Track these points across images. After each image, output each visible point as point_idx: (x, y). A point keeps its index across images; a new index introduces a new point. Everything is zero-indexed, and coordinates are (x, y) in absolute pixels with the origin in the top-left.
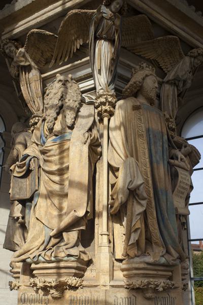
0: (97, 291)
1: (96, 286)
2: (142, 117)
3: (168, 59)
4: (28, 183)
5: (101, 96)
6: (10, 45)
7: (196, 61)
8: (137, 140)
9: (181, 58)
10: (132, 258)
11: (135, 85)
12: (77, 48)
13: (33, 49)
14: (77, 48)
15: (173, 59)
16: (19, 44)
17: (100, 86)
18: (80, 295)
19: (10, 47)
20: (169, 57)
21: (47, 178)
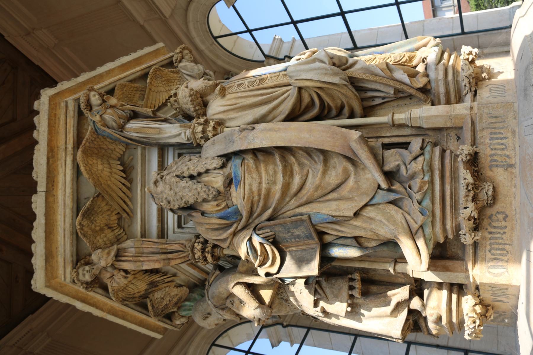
0: (481, 119)
1: (473, 123)
2: (236, 84)
4: (294, 249)
5: (194, 133)
6: (80, 271)
7: (187, 57)
8: (265, 85)
9: (178, 72)
10: (429, 81)
13: (98, 238)
15: (176, 81)
16: (85, 258)
17: (180, 134)
18: (489, 149)
19: (83, 270)
21: (293, 201)
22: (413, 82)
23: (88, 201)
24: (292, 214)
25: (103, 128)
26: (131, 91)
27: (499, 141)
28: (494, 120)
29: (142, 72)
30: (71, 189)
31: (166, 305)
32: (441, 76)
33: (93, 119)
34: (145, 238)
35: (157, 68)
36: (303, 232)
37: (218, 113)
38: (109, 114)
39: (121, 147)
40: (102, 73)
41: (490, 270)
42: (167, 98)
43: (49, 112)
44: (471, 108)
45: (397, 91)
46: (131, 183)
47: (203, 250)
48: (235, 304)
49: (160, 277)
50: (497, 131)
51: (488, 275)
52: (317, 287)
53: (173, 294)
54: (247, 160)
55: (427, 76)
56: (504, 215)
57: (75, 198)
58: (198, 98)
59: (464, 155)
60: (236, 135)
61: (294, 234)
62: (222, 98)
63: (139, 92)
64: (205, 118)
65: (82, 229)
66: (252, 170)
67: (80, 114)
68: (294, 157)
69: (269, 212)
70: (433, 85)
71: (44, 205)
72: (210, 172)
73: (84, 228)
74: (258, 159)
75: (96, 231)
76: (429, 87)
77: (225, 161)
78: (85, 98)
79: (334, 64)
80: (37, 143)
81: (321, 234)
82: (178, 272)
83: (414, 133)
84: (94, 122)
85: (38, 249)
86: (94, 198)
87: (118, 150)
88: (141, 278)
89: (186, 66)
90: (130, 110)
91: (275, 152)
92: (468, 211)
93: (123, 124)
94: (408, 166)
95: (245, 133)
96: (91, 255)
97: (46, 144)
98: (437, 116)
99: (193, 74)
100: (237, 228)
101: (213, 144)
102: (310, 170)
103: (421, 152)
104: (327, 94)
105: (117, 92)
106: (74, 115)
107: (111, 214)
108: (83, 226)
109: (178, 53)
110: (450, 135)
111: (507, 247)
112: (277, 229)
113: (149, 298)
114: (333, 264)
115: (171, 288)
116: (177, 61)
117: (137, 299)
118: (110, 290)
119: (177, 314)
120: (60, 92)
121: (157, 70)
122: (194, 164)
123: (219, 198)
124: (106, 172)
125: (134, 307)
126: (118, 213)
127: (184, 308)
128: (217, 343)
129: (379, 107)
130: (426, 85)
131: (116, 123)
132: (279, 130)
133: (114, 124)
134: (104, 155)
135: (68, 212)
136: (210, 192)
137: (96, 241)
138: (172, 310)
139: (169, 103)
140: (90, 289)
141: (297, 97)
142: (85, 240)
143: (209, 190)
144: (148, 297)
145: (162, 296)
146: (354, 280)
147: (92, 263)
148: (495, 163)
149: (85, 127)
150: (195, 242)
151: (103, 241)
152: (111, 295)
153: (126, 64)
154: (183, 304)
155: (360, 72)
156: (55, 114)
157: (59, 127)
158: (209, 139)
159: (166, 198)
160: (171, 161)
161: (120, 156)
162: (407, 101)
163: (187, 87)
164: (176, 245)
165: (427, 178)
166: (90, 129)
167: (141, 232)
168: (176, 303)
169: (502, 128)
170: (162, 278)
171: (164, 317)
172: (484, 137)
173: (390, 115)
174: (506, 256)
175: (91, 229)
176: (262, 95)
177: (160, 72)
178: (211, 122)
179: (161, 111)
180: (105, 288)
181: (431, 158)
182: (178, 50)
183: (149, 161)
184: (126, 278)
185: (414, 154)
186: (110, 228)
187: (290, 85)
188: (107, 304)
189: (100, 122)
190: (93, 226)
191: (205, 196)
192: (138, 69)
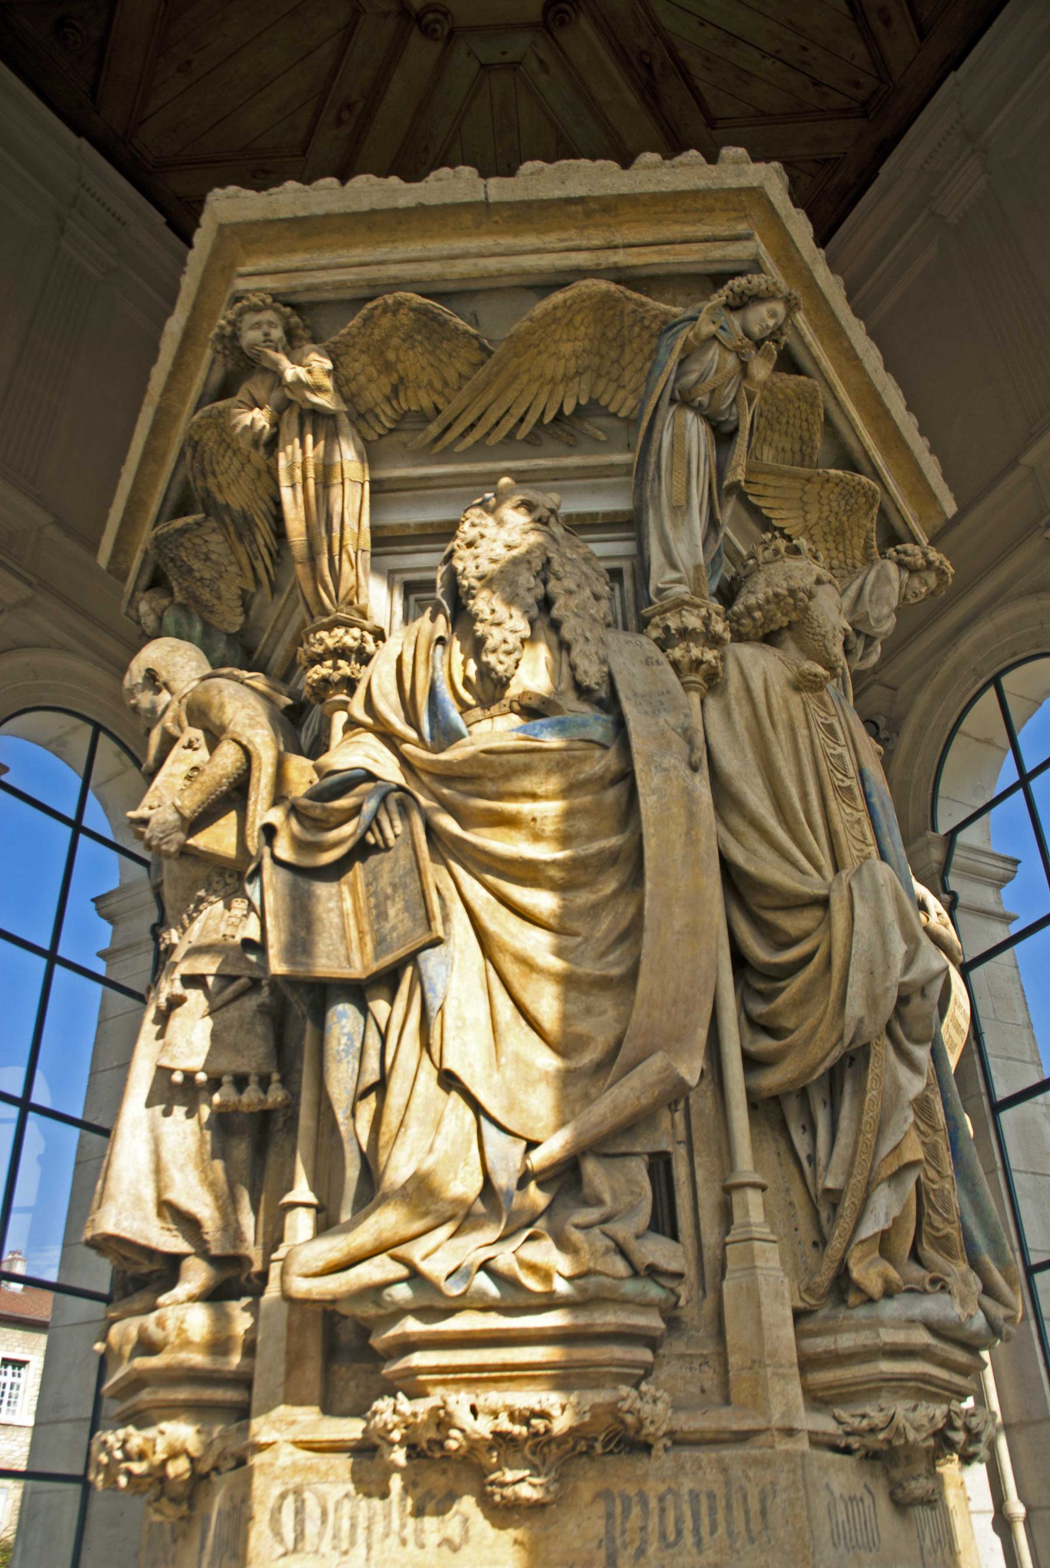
0: (756, 1462)
1: (743, 1437)
2: (834, 721)
3: (829, 550)
5: (679, 605)
6: (269, 316)
7: (916, 583)
8: (833, 805)
9: (868, 560)
10: (870, 1300)
11: (791, 601)
12: (561, 411)
13: (364, 358)
14: (561, 411)
15: (841, 556)
17: (674, 566)
18: (662, 1488)
19: (270, 324)
20: (831, 545)
22: (865, 1247)
23: (470, 323)
24: (444, 892)
25: (679, 345)
26: (797, 423)
27: (689, 1524)
28: (754, 1505)
29: (858, 454)
30: (498, 270)
31: (191, 570)
32: (889, 1336)
33: (702, 316)
34: (372, 492)
35: (873, 496)
36: (394, 928)
37: (742, 673)
38: (722, 361)
39: (631, 402)
40: (847, 339)
41: (291, 1498)
42: (786, 531)
43: (717, 191)
44: (790, 1432)
45: (834, 1198)
46: (525, 440)
47: (341, 653)
48: (189, 751)
49: (266, 545)
50: (720, 1515)
51: (276, 1491)
52: (243, 981)
53: (223, 587)
54: (602, 757)
55: (889, 1293)
56: (457, 1540)
57: (473, 286)
58: (786, 615)
59: (638, 1404)
60: (672, 721)
61: (389, 903)
62: (789, 682)
63: (797, 447)
64: (728, 636)
65: (385, 312)
66: (573, 771)
67: (718, 279)
68: (616, 894)
69: (448, 823)
70: (861, 1313)
71: (448, 200)
72: (564, 654)
73: (389, 315)
74: (605, 788)
75: (382, 352)
76: (852, 1299)
77: (597, 695)
78: (764, 287)
79: (903, 1000)
80: (626, 161)
81: (387, 981)
82: (284, 597)
83: (708, 1254)
84: (695, 319)
85: (326, 196)
86: (476, 337)
87: (621, 394)
88: (260, 491)
89: (889, 580)
90: (738, 419)
91: (627, 834)
92: (463, 1417)
93: (696, 404)
94: (596, 1231)
95: (679, 744)
96: (315, 342)
97: (624, 190)
98: (759, 1322)
99: (866, 606)
100: (405, 741)
101: (648, 662)
102: (579, 939)
103: (641, 1268)
104: (812, 983)
105: (791, 381)
106: (712, 262)
107: (435, 391)
108: (395, 313)
109: (925, 555)
110: (705, 1368)
111: (360, 1550)
112: (403, 854)
113: (206, 519)
114: (309, 1026)
115: (238, 581)
116: (902, 556)
117: (200, 483)
118: (220, 404)
119: (165, 602)
120: (778, 216)
121: (869, 496)
122: (584, 608)
123: (489, 686)
124: (554, 368)
125: (179, 477)
126: (438, 411)
127: (184, 621)
128: (103, 738)
129: (783, 1146)
130: (859, 1289)
131: (697, 382)
132: (691, 839)
133: (693, 377)
134: (602, 357)
135: (433, 269)
136: (503, 657)
137: (355, 352)
138: (176, 589)
139: (770, 535)
140: (219, 347)
141: (798, 896)
142: (356, 321)
143: (509, 653)
144: (208, 515)
145: (213, 557)
146: (265, 1092)
147: (293, 348)
148: (618, 1510)
149: (681, 298)
150: (363, 629)
151: (356, 374)
152: (206, 408)
153: (882, 405)
154: (196, 617)
155: (886, 1080)
156: (711, 210)
157: (676, 222)
158: (664, 651)
159: (482, 536)
160: (598, 549)
161: (603, 403)
162: (806, 1233)
163: (819, 581)
164: (353, 579)
165: (561, 1287)
166: (675, 310)
167: (389, 480)
168: (197, 600)
169: (730, 1533)
170: (264, 551)
171: (157, 568)
172: (702, 1471)
173: (757, 1178)
174: (334, 1548)
175: (389, 336)
176: (804, 796)
177: (866, 507)
178: (715, 652)
179: (744, 515)
180: (226, 390)
181: (623, 1302)
182: (934, 555)
183: (596, 490)
184: (256, 444)
185: (633, 1245)
186: (395, 390)
187: (837, 869)
188: (183, 402)
189: (696, 336)
190: (395, 341)
191: (490, 643)
192: (869, 441)
